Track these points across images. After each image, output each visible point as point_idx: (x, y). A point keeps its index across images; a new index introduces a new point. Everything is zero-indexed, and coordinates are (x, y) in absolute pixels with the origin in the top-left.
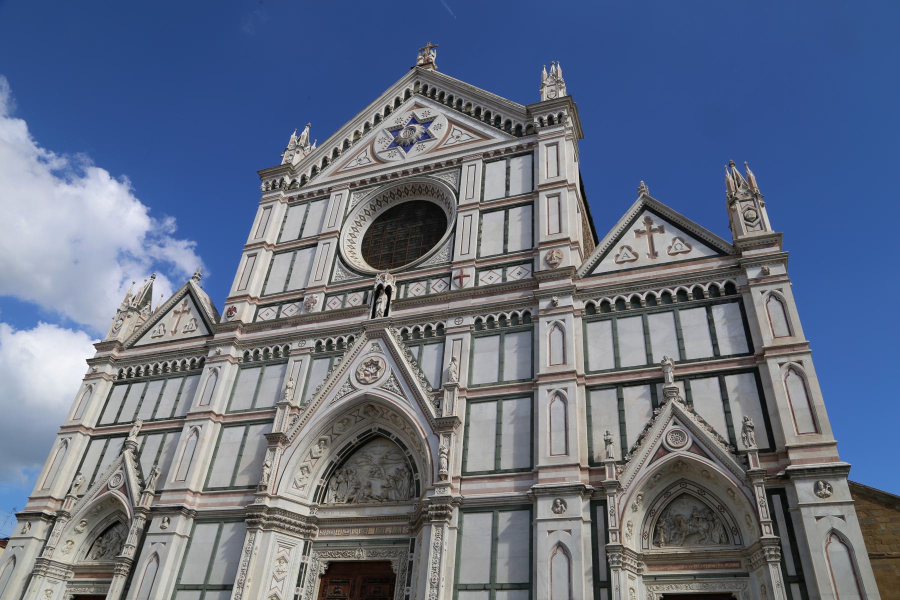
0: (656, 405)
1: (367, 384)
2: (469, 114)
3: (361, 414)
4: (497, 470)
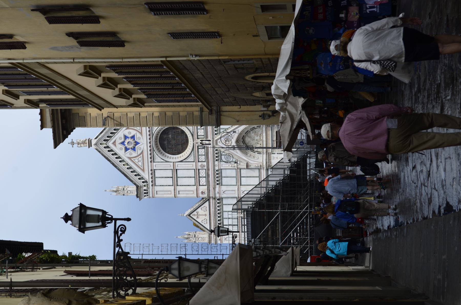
1: (232, 142)
3: (239, 144)
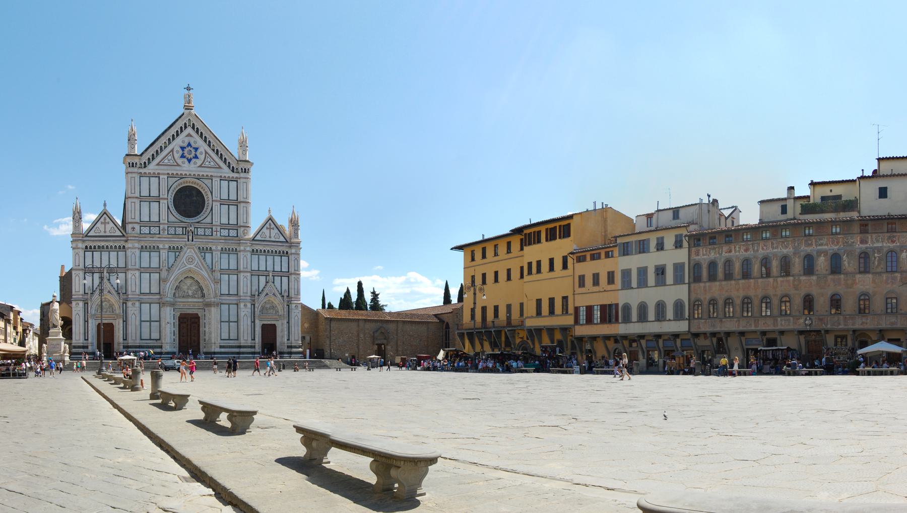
0: (267, 282)
2: (214, 150)
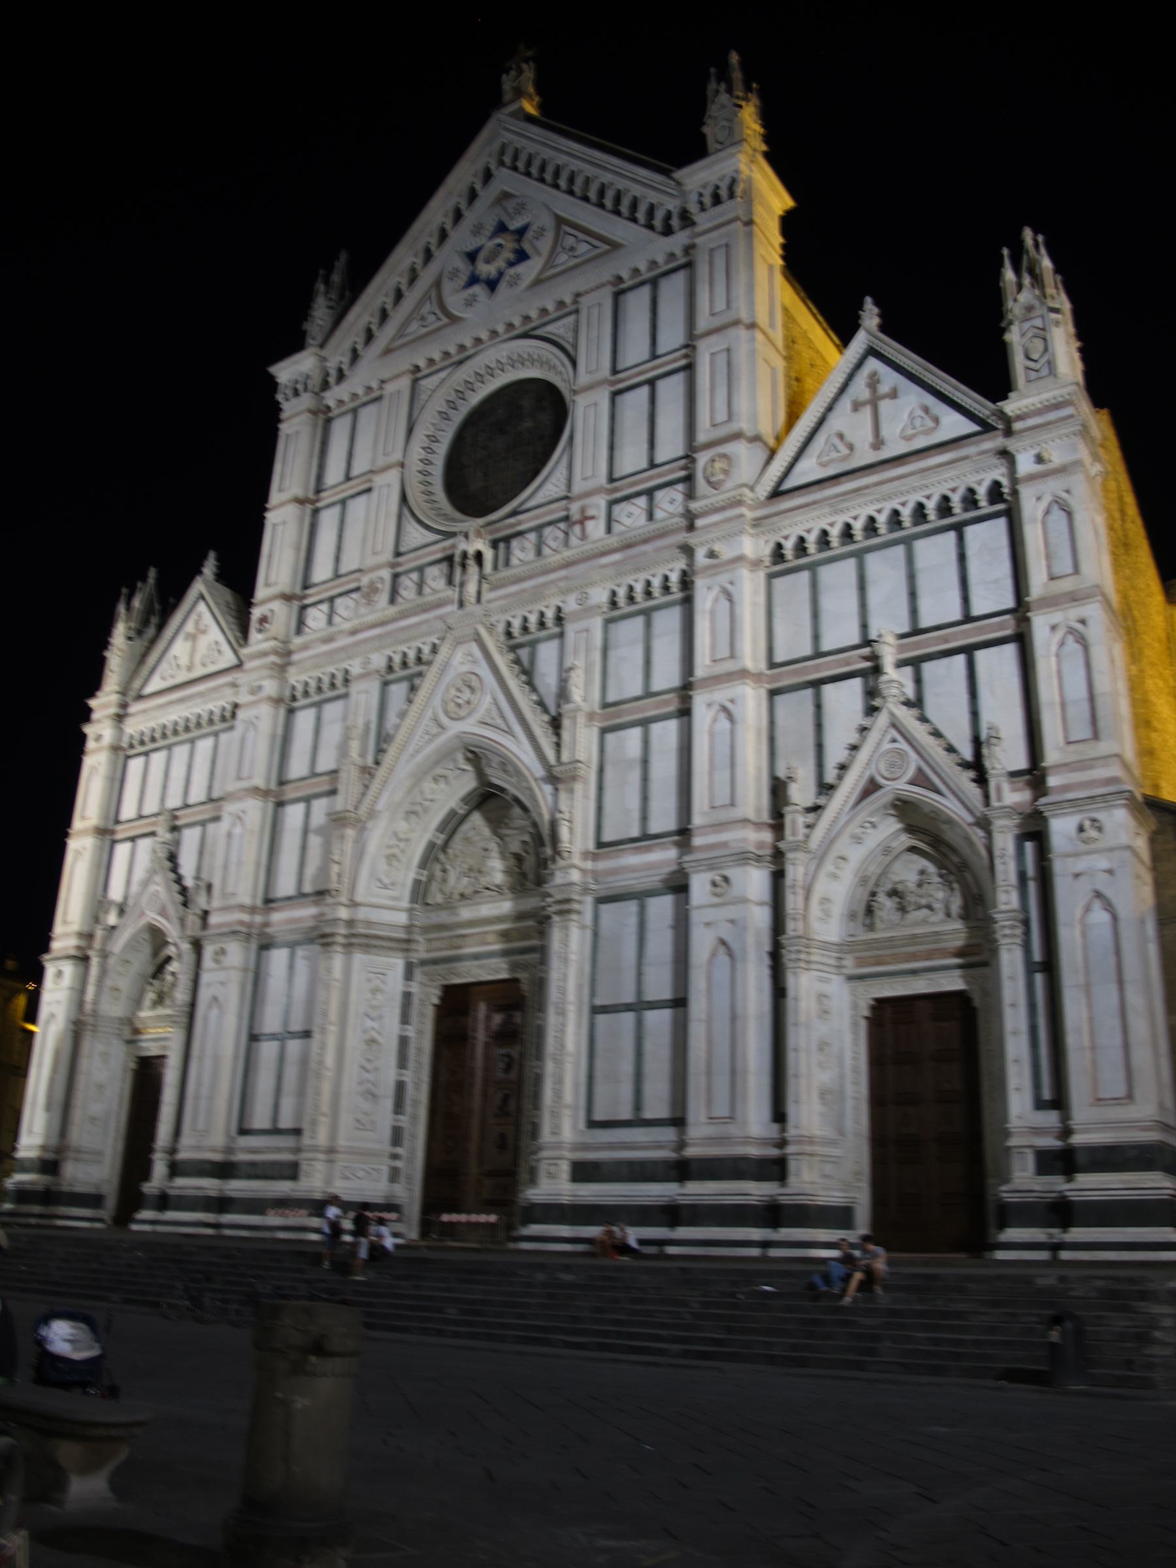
0: (871, 711)
4: (645, 837)
